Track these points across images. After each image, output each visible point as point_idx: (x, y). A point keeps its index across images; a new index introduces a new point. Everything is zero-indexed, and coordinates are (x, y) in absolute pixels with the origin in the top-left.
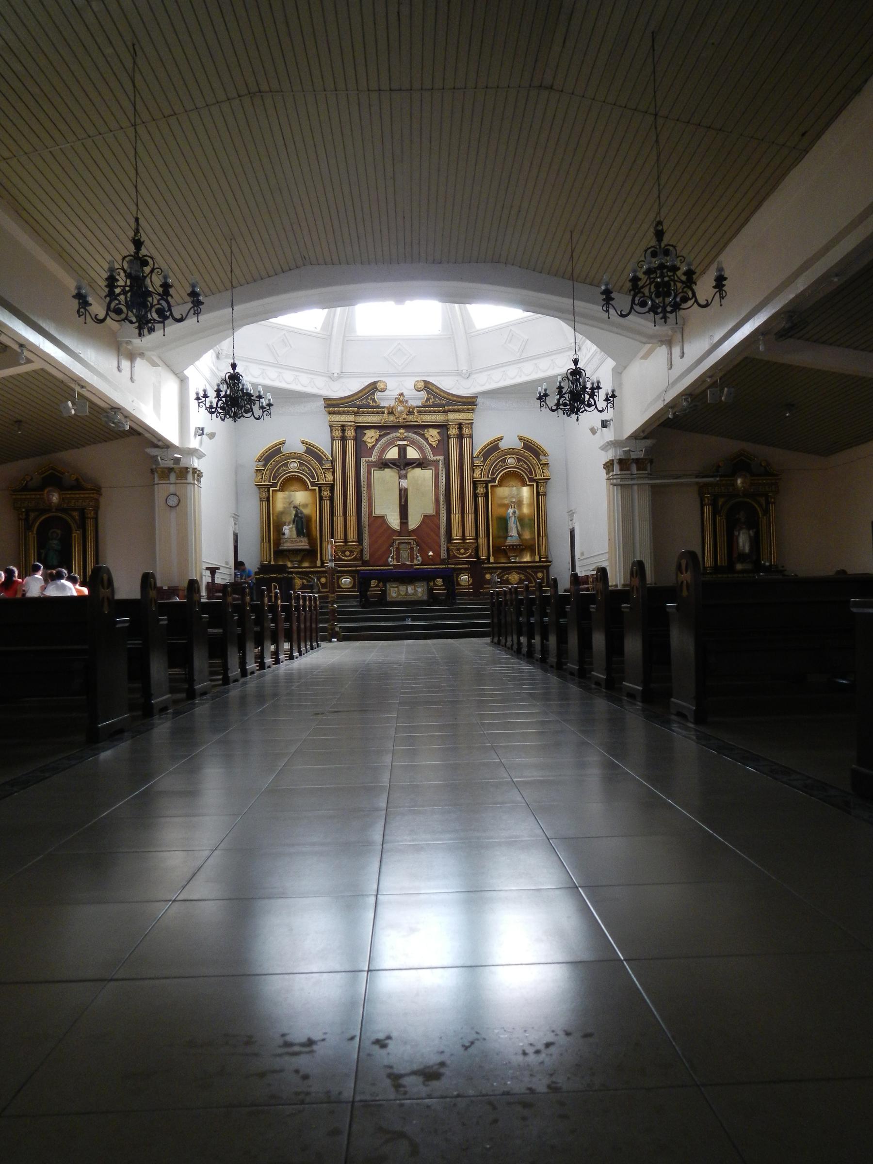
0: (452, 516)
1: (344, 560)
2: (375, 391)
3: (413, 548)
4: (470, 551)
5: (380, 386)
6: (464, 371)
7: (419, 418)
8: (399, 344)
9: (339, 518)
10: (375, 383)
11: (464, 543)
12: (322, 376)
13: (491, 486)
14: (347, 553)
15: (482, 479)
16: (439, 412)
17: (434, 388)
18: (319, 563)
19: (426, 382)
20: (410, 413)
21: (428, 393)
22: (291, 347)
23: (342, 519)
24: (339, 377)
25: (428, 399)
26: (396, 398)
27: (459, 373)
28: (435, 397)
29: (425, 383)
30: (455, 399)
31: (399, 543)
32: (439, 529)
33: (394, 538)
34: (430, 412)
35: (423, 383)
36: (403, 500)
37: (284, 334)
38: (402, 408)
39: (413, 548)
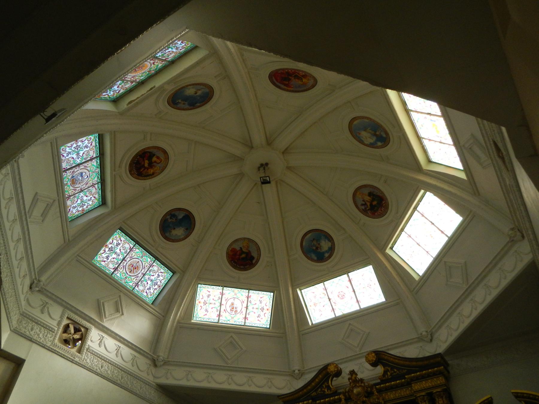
2: (329, 377)
5: (332, 368)
6: (424, 333)
7: (381, 398)
8: (350, 324)
10: (326, 367)
12: (281, 375)
16: (402, 386)
17: (386, 357)
19: (377, 353)
20: (369, 394)
21: (384, 365)
22: (242, 349)
24: (302, 374)
25: (385, 372)
26: (349, 379)
27: (420, 339)
28: (392, 368)
29: (376, 354)
30: (414, 363)
34: (392, 388)
35: (373, 354)
37: (231, 336)
38: (359, 389)
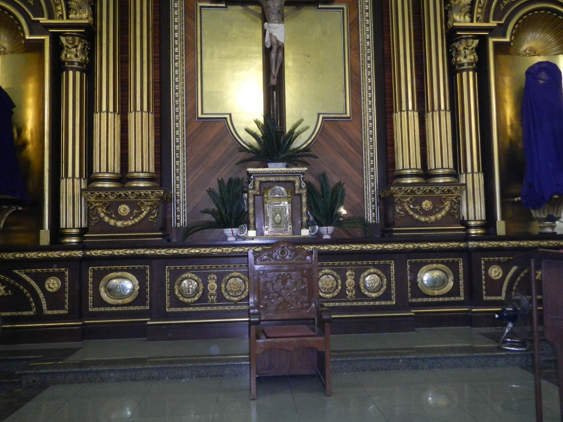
0: (397, 116)
1: (115, 229)
3: (300, 195)
4: (447, 204)
9: (104, 115)
11: (427, 184)
13: (495, 44)
14: (124, 209)
15: (475, 24)
18: (45, 237)
23: (114, 121)
31: (261, 182)
32: (360, 151)
33: (250, 170)
36: (274, 72)
39: (300, 195)
